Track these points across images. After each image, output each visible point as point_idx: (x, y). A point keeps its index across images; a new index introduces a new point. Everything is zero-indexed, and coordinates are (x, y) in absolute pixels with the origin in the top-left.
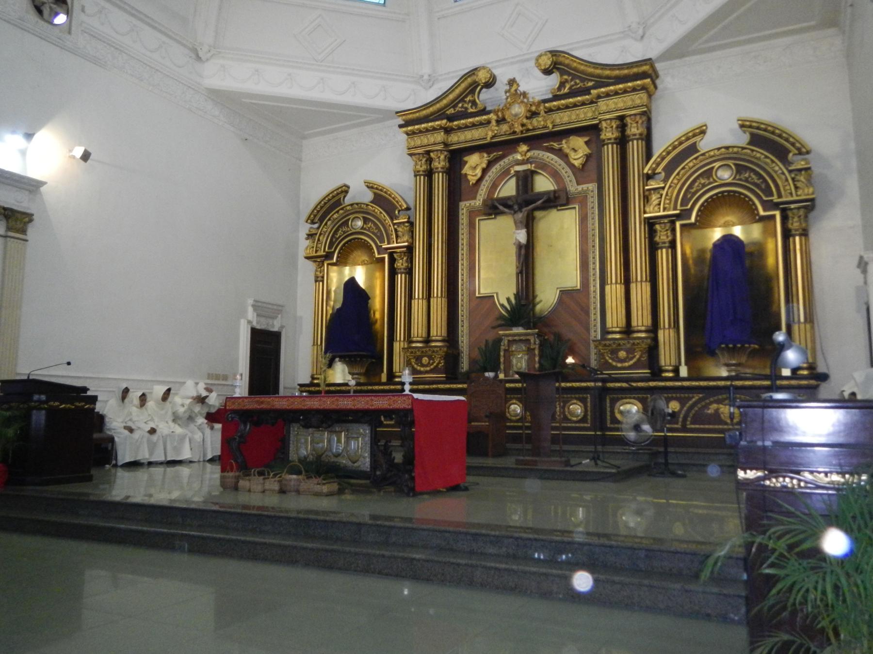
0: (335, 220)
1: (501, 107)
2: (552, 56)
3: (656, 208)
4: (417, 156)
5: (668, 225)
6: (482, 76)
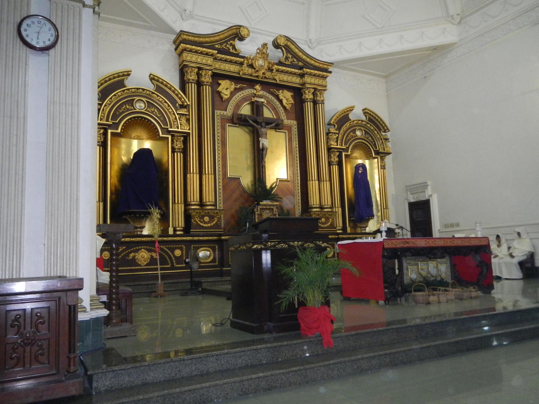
0: (119, 96)
1: (252, 57)
2: (287, 39)
3: (336, 144)
4: (193, 69)
5: (338, 153)
6: (244, 32)
